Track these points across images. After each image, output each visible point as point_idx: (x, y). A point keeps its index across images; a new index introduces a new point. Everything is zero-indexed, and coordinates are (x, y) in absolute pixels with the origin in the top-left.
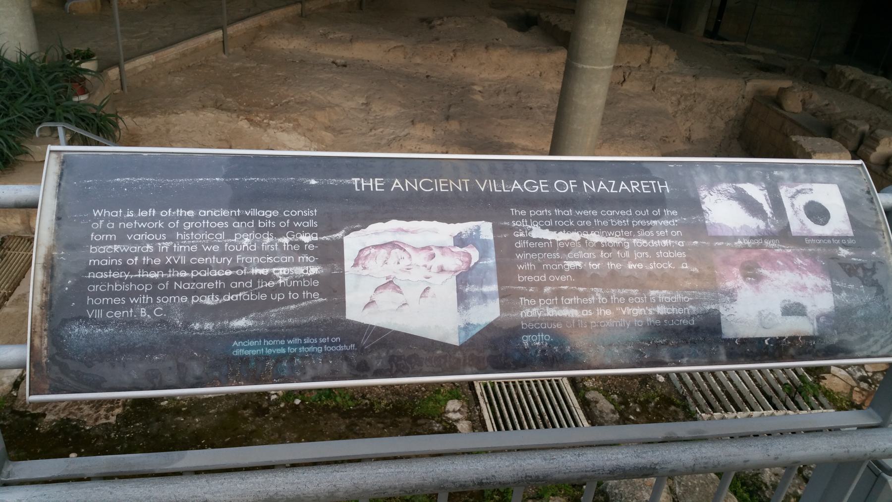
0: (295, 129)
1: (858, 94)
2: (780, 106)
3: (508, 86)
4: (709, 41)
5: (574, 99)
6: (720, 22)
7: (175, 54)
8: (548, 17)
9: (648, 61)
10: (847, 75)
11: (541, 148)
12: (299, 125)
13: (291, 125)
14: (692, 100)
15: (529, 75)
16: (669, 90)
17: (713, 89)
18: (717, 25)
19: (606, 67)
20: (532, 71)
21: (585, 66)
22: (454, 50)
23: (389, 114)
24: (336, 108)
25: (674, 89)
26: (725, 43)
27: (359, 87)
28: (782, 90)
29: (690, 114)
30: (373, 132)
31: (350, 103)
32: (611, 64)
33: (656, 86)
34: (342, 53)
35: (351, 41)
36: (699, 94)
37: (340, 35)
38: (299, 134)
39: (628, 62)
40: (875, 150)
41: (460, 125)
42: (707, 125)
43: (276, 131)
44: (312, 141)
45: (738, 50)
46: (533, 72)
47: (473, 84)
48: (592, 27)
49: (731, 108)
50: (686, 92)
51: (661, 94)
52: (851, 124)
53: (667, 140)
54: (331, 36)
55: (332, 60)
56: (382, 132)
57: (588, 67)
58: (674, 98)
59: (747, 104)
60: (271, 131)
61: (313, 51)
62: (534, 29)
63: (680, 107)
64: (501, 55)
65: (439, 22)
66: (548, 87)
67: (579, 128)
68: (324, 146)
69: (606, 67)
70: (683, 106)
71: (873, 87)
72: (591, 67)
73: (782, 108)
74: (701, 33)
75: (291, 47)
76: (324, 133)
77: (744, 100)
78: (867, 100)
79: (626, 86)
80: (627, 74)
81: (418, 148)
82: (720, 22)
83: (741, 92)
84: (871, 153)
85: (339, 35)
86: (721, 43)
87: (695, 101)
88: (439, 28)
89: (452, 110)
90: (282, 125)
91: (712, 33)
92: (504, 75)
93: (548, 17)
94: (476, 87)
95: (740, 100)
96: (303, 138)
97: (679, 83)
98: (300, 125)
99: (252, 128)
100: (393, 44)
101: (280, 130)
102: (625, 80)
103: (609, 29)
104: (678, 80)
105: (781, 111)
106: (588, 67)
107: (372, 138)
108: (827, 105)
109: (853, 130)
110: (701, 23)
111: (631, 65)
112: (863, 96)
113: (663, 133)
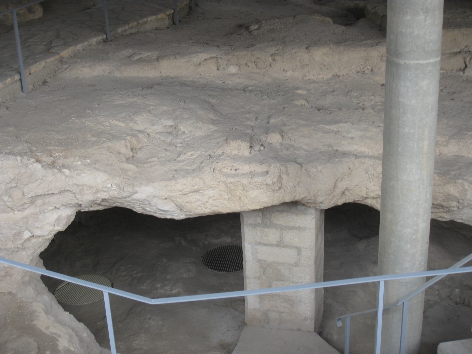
3: (336, 86)
5: (400, 99)
8: (375, 8)
19: (432, 60)
20: (362, 67)
22: (272, 55)
23: (199, 133)
24: (140, 135)
27: (166, 108)
30: (182, 157)
31: (155, 127)
32: (437, 57)
35: (157, 59)
37: (145, 55)
41: (283, 137)
47: (298, 88)
48: (409, 17)
54: (136, 58)
62: (362, 22)
65: (256, 27)
67: (412, 131)
69: (432, 60)
80: (468, 59)
85: (145, 54)
88: (256, 33)
89: (272, 121)
93: (375, 8)
94: (299, 92)
100: (203, 56)
102: (466, 66)
103: (428, 18)
107: (181, 164)
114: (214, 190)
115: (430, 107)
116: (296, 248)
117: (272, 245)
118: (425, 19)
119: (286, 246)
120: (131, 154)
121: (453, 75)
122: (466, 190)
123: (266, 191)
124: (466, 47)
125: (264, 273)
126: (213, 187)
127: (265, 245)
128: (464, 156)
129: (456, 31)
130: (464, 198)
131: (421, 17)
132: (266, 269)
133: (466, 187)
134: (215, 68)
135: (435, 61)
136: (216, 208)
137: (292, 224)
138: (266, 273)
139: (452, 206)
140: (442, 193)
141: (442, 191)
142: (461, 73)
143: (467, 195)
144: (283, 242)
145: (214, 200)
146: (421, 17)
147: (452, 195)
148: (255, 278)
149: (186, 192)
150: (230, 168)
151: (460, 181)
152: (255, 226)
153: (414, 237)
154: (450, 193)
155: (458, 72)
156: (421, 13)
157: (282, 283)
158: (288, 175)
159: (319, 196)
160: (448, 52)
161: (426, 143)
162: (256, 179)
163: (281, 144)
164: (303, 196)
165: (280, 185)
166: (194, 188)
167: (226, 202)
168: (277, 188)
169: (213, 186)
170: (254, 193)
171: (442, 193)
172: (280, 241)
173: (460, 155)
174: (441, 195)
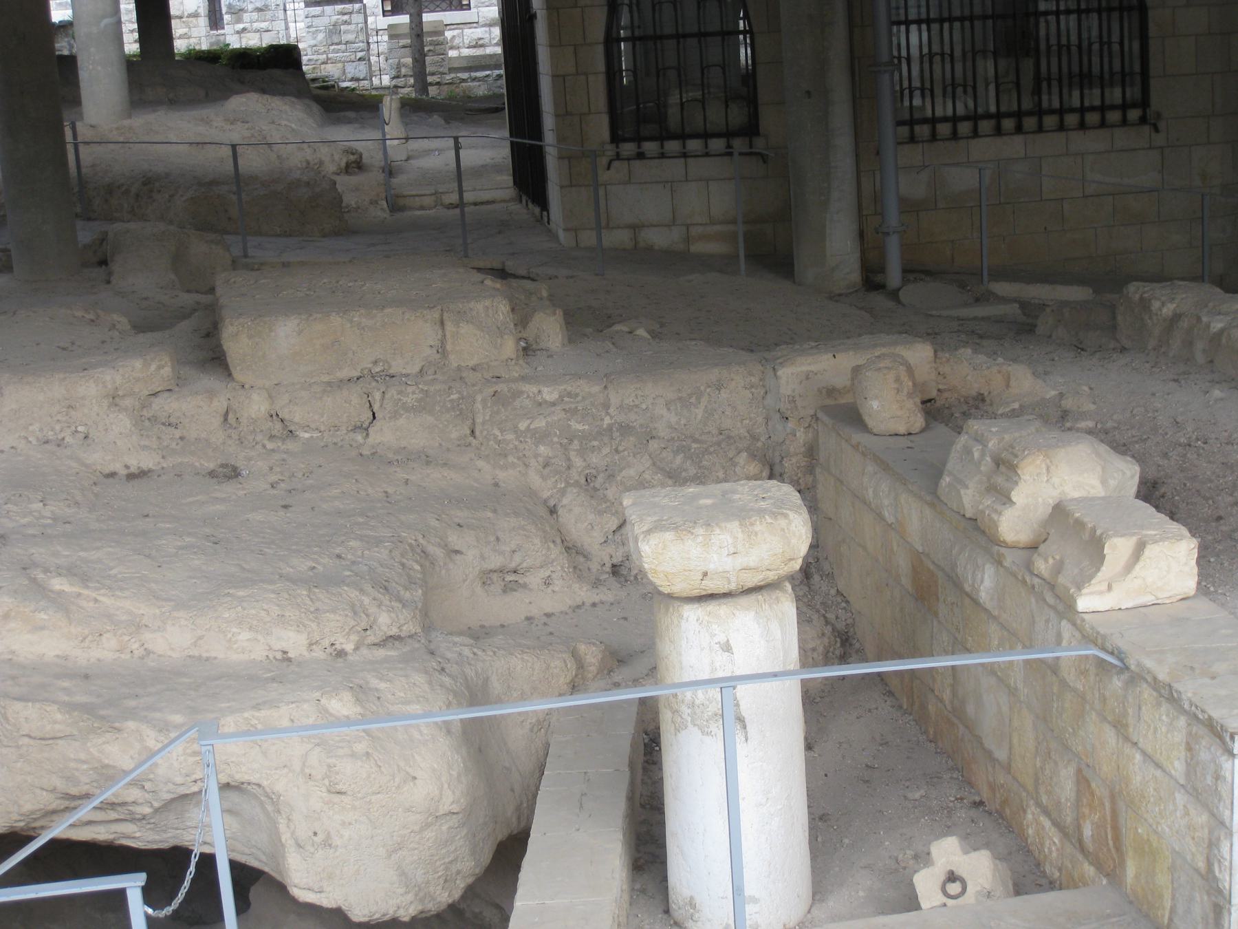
9: (442, 350)
10: (1156, 305)
16: (523, 426)
17: (668, 405)
20: (58, 427)
25: (540, 423)
33: (479, 420)
36: (626, 429)
51: (499, 442)
79: (384, 435)
83: (769, 400)
87: (617, 451)
97: (554, 404)
105: (858, 437)
112: (1200, 358)
113: (483, 558)
121: (335, 444)
124: (375, 363)
128: (216, 658)
129: (336, 320)
130: (152, 776)
139: (130, 799)
140: (84, 762)
141: (83, 756)
142: (359, 438)
147: (114, 767)
151: (131, 725)
154: (106, 762)
155: (352, 435)
160: (326, 378)
171: (84, 762)
173: (205, 655)
174: (85, 767)
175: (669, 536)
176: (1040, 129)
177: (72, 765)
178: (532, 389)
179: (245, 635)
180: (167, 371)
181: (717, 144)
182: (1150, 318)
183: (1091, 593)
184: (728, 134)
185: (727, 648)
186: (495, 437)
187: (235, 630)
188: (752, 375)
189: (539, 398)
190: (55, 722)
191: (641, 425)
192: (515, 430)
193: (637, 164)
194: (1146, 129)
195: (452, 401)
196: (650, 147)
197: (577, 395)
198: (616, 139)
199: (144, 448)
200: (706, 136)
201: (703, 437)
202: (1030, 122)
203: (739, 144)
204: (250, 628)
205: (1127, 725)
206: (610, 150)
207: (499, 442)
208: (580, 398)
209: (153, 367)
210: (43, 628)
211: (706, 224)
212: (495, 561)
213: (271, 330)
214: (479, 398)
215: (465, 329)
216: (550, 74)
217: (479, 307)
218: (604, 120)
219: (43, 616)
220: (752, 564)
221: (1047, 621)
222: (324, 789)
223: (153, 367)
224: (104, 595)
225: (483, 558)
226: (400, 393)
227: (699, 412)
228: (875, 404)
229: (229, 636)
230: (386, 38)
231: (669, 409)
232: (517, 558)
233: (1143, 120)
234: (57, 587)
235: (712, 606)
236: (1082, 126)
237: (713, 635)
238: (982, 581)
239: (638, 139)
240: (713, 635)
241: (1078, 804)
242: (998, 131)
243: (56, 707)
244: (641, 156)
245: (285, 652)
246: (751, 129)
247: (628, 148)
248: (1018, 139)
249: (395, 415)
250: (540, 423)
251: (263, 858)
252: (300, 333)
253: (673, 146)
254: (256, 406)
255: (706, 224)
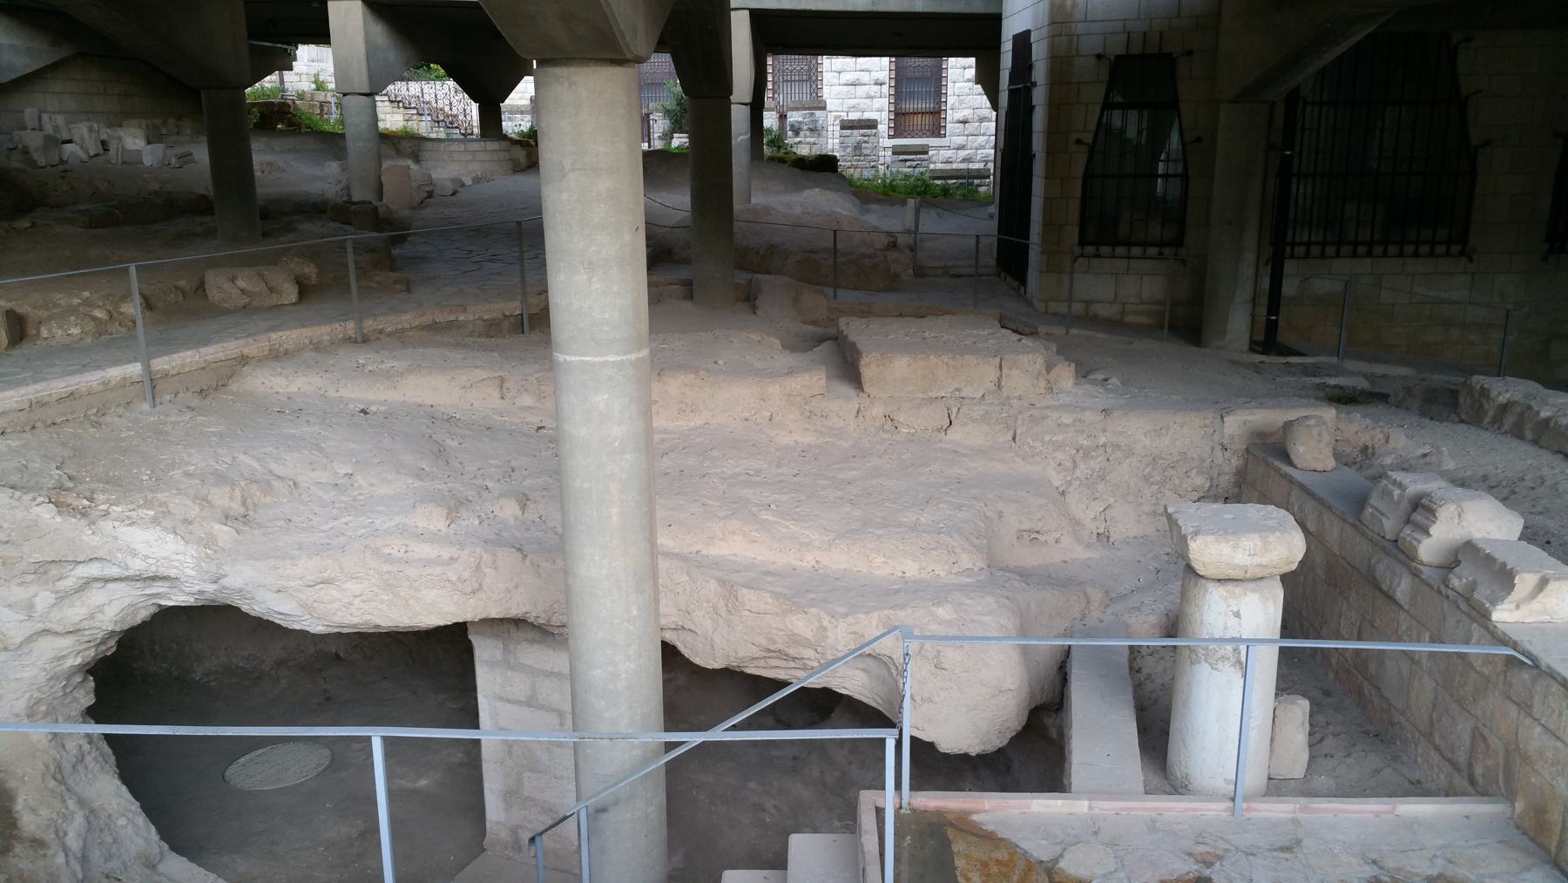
0: (155, 521)
1: (1518, 434)
2: (1286, 457)
4: (1257, 358)
6: (1277, 320)
7: (16, 402)
10: (1494, 393)
11: (694, 549)
12: (167, 513)
13: (151, 513)
14: (1100, 459)
15: (746, 420)
16: (1047, 438)
17: (1145, 434)
18: (1272, 328)
20: (753, 412)
21: (568, 358)
23: (384, 490)
25: (1059, 438)
26: (1293, 360)
28: (1288, 425)
29: (1101, 487)
33: (1018, 432)
34: (378, 395)
36: (1116, 446)
37: (389, 365)
38: (165, 529)
39: (958, 390)
40: (1426, 532)
41: (523, 508)
42: (1147, 508)
43: (116, 524)
44: (187, 543)
45: (1313, 371)
46: (755, 414)
49: (1195, 471)
50: (1083, 441)
51: (1031, 447)
52: (1395, 482)
53: (1042, 538)
55: (362, 407)
56: (346, 524)
57: (574, 358)
58: (1060, 455)
59: (1236, 462)
60: (106, 526)
61: (332, 393)
63: (1078, 473)
64: (686, 385)
66: (784, 439)
68: (209, 552)
70: (1083, 470)
71: (1544, 414)
72: (578, 358)
73: (1291, 463)
74: (1244, 343)
75: (293, 388)
76: (217, 527)
77: (1227, 454)
78: (1535, 442)
79: (955, 434)
80: (955, 410)
81: (402, 551)
82: (1277, 320)
83: (1216, 437)
84: (1419, 542)
85: (388, 364)
86: (1282, 360)
87: (1108, 460)
90: (133, 514)
91: (1268, 341)
92: (698, 421)
95: (1219, 453)
96: (172, 536)
97: (1068, 426)
98: (169, 512)
99: (58, 519)
100: (480, 374)
101: (127, 522)
103: (595, 280)
104: (1067, 419)
106: (574, 358)
108: (1425, 455)
109: (1397, 492)
110: (1238, 324)
111: (963, 394)
112: (1529, 435)
114: (362, 583)
115: (617, 444)
116: (557, 711)
117: (519, 703)
118: (589, 281)
119: (542, 707)
120: (242, 510)
122: (825, 629)
123: (450, 593)
125: (510, 753)
126: (356, 578)
127: (509, 701)
131: (582, 277)
132: (512, 746)
133: (825, 623)
134: (496, 394)
135: (619, 359)
136: (365, 617)
137: (548, 667)
138: (512, 755)
139: (806, 657)
140: (781, 630)
141: (781, 626)
143: (827, 637)
144: (537, 699)
145: (364, 601)
146: (582, 277)
148: (495, 763)
149: (310, 581)
150: (396, 548)
152: (493, 664)
153: (611, 687)
156: (581, 268)
157: (539, 775)
158: (496, 569)
159: (555, 613)
160: (921, 396)
161: (615, 510)
162: (429, 570)
163: (516, 518)
164: (524, 610)
165: (476, 586)
166: (322, 575)
167: (384, 607)
168: (469, 590)
169: (358, 575)
170: (430, 595)
171: (781, 630)
172: (532, 696)
174: (782, 633)
175: (1210, 538)
176: (1385, 255)
177: (774, 631)
178: (1055, 415)
179: (880, 560)
180: (823, 382)
181: (1152, 251)
182: (1488, 402)
183: (1504, 610)
184: (1161, 244)
185: (1237, 615)
186: (1029, 443)
187: (874, 555)
188: (1205, 418)
189: (1059, 421)
190: (767, 604)
191: (1126, 445)
192: (1042, 441)
193: (1094, 261)
194: (1464, 259)
195: (1002, 418)
196: (1105, 250)
197: (1084, 421)
198: (1083, 242)
199: (806, 429)
200: (1145, 245)
201: (1168, 457)
202: (1378, 250)
203: (1167, 251)
204: (884, 556)
205: (1532, 706)
206: (1077, 250)
207: (1031, 447)
208: (1086, 423)
209: (815, 379)
210: (755, 542)
211: (1138, 304)
212: (1027, 525)
213: (891, 362)
214: (1020, 417)
215: (1015, 372)
216: (1043, 196)
217: (1024, 359)
218: (1076, 230)
219: (756, 534)
220: (1264, 563)
221: (1458, 622)
222: (933, 666)
223: (815, 379)
224: (793, 525)
225: (1020, 522)
226: (969, 410)
227: (1166, 440)
228: (1301, 449)
229: (871, 558)
230: (890, 153)
231: (1146, 436)
232: (1040, 524)
233: (1462, 253)
234: (764, 517)
235: (1230, 587)
236: (1416, 255)
237: (1228, 606)
238: (1399, 584)
239: (1098, 244)
240: (1228, 606)
241: (1473, 749)
242: (1354, 255)
243: (769, 594)
244: (1098, 256)
245: (904, 573)
246: (1178, 242)
247: (1090, 249)
248: (1368, 261)
249: (965, 425)
250: (1059, 438)
251: (881, 702)
252: (909, 365)
253: (1121, 250)
254: (878, 410)
255: (1138, 304)
